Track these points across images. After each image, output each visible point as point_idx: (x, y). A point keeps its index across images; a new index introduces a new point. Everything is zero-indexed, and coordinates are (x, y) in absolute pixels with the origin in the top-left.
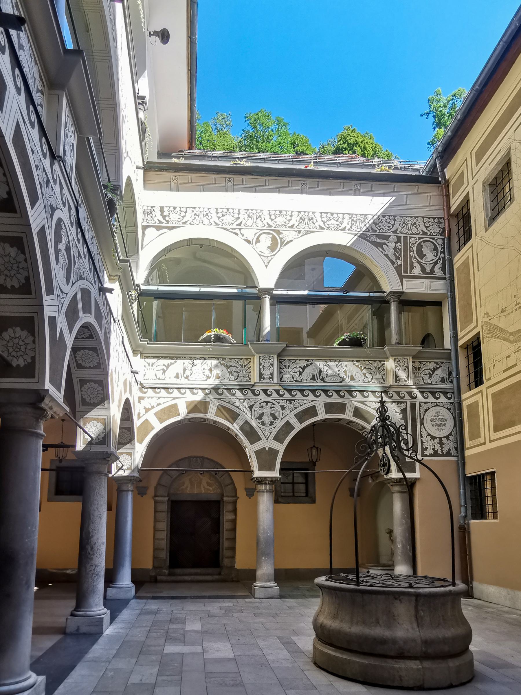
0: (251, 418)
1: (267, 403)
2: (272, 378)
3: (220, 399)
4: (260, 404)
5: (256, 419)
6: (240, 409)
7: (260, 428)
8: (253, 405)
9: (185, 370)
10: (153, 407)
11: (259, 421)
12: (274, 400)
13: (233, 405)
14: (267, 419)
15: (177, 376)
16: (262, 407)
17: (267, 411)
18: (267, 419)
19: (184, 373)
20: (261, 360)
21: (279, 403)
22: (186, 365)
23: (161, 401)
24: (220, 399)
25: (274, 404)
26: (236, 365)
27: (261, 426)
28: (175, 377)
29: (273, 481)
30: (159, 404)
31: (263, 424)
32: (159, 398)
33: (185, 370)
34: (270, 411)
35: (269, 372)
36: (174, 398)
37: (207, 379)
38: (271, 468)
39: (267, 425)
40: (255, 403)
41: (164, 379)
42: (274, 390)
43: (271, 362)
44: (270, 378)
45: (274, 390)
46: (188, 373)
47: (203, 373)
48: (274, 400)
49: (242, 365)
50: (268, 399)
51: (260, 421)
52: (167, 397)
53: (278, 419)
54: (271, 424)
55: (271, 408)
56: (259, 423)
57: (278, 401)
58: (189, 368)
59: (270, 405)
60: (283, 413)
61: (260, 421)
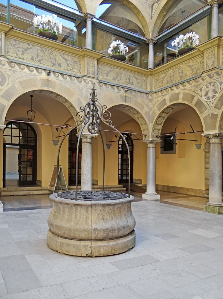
0: (201, 97)
1: (210, 83)
2: (214, 64)
3: (185, 89)
4: (206, 85)
5: (204, 96)
6: (195, 92)
7: (206, 101)
8: (202, 87)
9: (171, 77)
10: (156, 103)
11: (205, 97)
12: (215, 80)
13: (191, 91)
14: (210, 94)
15: (167, 83)
16: (208, 87)
17: (211, 88)
18: (210, 94)
19: (170, 79)
20: (207, 54)
21: (218, 81)
22: (171, 74)
23: (159, 98)
24: (185, 89)
25: (215, 83)
26: (196, 64)
27: (207, 100)
28: (166, 83)
29: (215, 136)
30: (159, 100)
31: (208, 98)
32: (158, 97)
33: (171, 77)
34: (212, 88)
35: (212, 61)
36: (164, 96)
37: (181, 78)
38: (214, 128)
39: (211, 99)
40: (203, 86)
41: (162, 86)
42: (215, 72)
43: (213, 54)
44: (212, 65)
45: (215, 72)
46: (172, 79)
47: (179, 75)
48: (215, 80)
49: (199, 63)
50: (212, 80)
51: (206, 97)
52: (161, 96)
53: (218, 92)
54: (213, 97)
55: (213, 86)
56: (205, 98)
57: (217, 80)
58: (173, 75)
59: (212, 84)
60: (221, 88)
61: (206, 97)
